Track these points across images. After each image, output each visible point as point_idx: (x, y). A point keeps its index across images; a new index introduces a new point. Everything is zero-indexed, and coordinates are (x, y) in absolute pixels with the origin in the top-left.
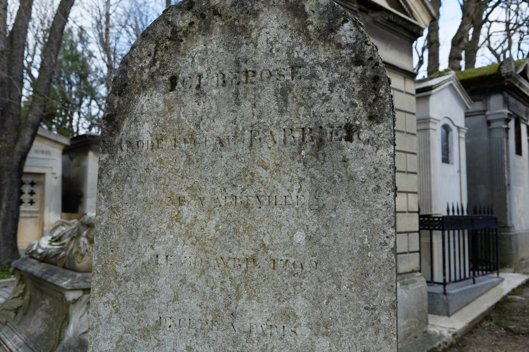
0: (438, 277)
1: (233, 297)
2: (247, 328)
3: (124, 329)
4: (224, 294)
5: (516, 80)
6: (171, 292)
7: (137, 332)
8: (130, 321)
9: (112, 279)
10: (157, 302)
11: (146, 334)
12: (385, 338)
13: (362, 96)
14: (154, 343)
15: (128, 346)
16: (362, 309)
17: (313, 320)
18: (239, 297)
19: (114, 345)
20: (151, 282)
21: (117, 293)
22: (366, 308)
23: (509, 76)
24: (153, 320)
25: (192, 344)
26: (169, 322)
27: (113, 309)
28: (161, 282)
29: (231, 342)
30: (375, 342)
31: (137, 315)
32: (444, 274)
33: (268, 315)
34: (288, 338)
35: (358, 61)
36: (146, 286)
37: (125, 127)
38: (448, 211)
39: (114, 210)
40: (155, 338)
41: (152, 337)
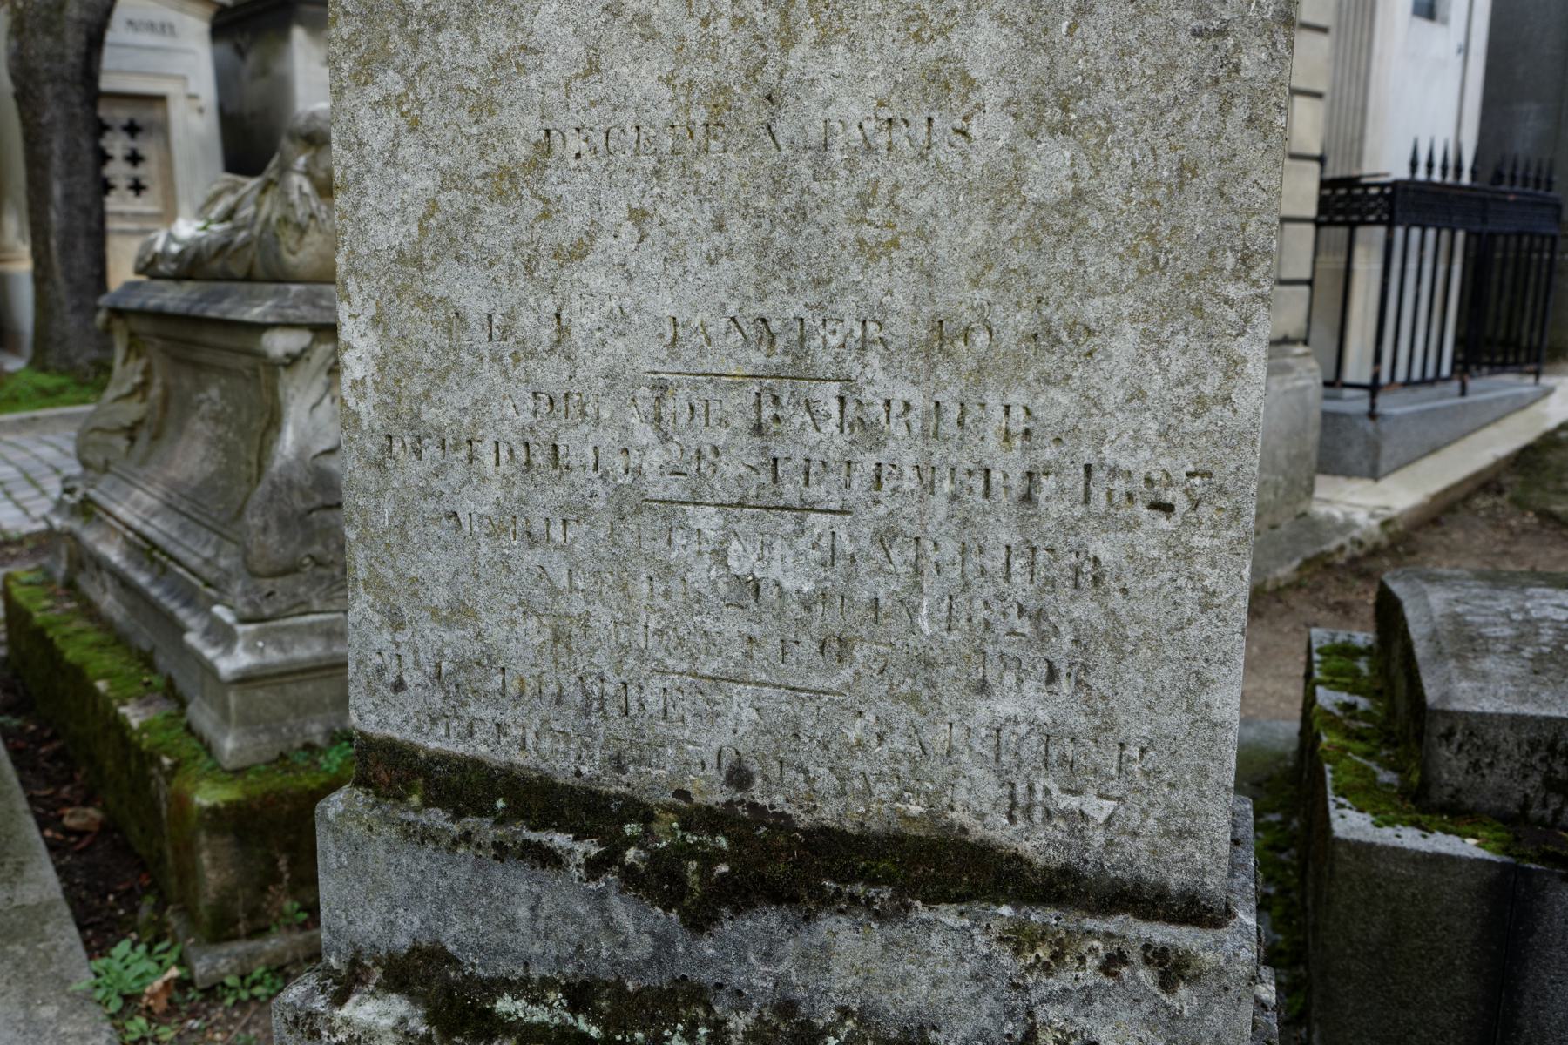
0: (1357, 368)
1: (772, 43)
2: (815, 134)
3: (439, 178)
4: (744, 35)
6: (576, 49)
7: (479, 183)
8: (457, 152)
9: (392, 26)
10: (534, 84)
11: (506, 185)
12: (1250, 121)
14: (531, 209)
15: (453, 226)
16: (1183, 37)
17: (1023, 86)
18: (789, 40)
19: (415, 230)
20: (514, 24)
21: (410, 71)
22: (1196, 33)
24: (526, 140)
25: (647, 201)
26: (575, 144)
27: (402, 122)
29: (766, 185)
30: (1214, 139)
31: (475, 130)
32: (1377, 359)
33: (882, 87)
34: (942, 153)
36: (497, 38)
38: (1414, 165)
40: (535, 195)
41: (526, 192)
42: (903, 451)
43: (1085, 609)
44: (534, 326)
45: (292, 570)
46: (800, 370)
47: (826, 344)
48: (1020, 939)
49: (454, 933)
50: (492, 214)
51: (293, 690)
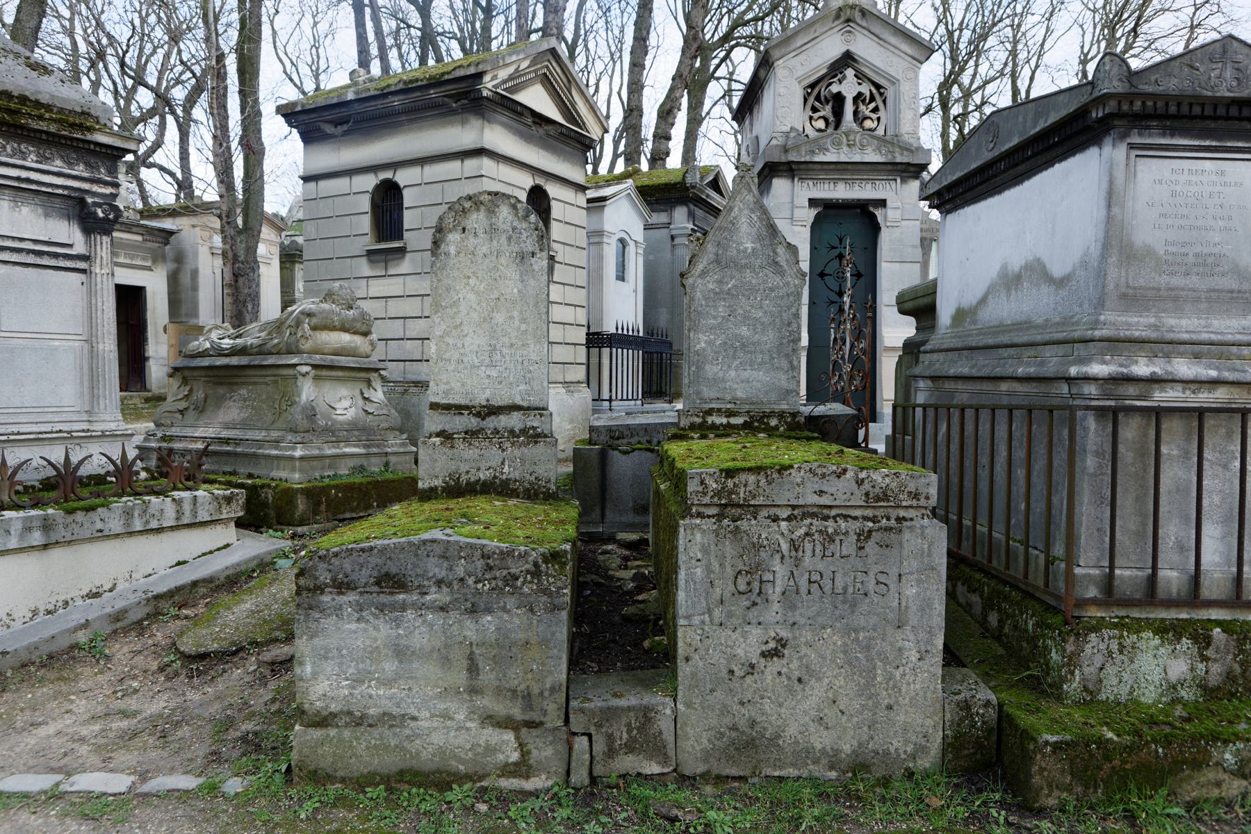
0: (606, 395)
5: (703, 192)
13: (538, 242)
23: (694, 187)
32: (611, 391)
35: (536, 229)
36: (455, 310)
37: (442, 247)
38: (617, 329)
39: (439, 281)
42: (508, 358)
43: (529, 375)
44: (460, 345)
45: (308, 431)
46: (495, 349)
47: (498, 346)
48: (524, 415)
50: (454, 331)
51: (312, 463)
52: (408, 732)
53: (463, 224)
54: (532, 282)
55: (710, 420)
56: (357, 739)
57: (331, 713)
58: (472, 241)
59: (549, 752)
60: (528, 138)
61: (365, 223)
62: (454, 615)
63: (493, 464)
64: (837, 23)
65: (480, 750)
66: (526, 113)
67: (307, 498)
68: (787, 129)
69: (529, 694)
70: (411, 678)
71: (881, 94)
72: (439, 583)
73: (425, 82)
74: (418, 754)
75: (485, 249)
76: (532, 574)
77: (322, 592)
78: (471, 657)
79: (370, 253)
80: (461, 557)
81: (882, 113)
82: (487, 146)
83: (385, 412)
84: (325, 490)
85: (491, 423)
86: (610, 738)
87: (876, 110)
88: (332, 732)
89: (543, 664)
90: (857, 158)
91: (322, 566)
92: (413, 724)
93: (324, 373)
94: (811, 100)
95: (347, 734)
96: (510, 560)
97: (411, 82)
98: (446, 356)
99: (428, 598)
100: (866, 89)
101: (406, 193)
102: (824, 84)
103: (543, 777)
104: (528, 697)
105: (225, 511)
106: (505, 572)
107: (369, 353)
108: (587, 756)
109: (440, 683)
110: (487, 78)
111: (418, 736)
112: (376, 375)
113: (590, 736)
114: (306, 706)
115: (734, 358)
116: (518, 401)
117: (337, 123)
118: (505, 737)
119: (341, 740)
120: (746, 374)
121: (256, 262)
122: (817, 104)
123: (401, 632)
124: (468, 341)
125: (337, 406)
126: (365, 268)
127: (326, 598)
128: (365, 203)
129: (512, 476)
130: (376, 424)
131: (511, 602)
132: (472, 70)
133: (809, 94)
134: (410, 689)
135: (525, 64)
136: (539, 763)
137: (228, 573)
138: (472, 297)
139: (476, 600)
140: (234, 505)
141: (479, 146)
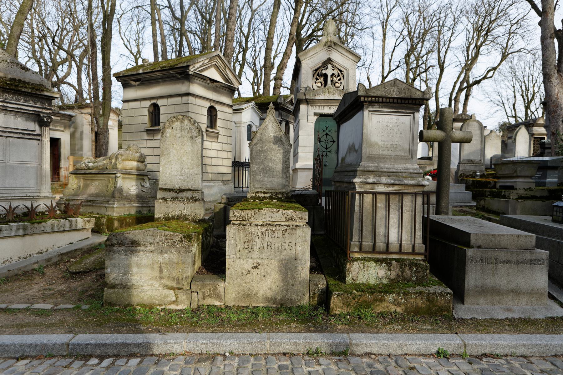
5: (285, 106)
28: (171, 155)
32: (243, 184)
44: (170, 168)
47: (184, 168)
49: (165, 196)
52: (140, 290)
53: (172, 126)
54: (196, 147)
55: (258, 195)
56: (124, 292)
57: (116, 284)
58: (175, 132)
59: (184, 297)
60: (208, 88)
61: (146, 119)
62: (155, 254)
63: (181, 209)
64: (325, 47)
65: (163, 296)
66: (207, 79)
67: (118, 221)
68: (306, 86)
69: (178, 279)
70: (141, 273)
71: (342, 74)
72: (151, 244)
73: (168, 68)
74: (143, 297)
75: (179, 135)
76: (180, 241)
77: (114, 246)
78: (160, 267)
79: (147, 131)
80: (158, 236)
81: (342, 81)
82: (191, 92)
83: (149, 191)
84: (125, 219)
85: (180, 195)
86: (204, 293)
87: (340, 80)
88: (116, 290)
89: (183, 270)
90: (332, 98)
91: (114, 238)
92: (142, 288)
93: (127, 176)
94: (316, 75)
95: (121, 291)
96: (173, 237)
97: (163, 67)
98: (165, 172)
99: (147, 248)
100: (336, 72)
101: (161, 108)
102: (321, 69)
103: (183, 305)
104: (178, 280)
105: (87, 225)
106: (171, 241)
107: (144, 169)
108: (197, 299)
109: (151, 275)
110: (191, 67)
111: (143, 292)
112: (146, 177)
113: (197, 292)
114: (108, 282)
115: (266, 173)
116: (190, 187)
117: (135, 81)
118: (171, 292)
119: (119, 293)
120: (270, 179)
121: (107, 129)
122: (318, 77)
123: (138, 259)
124: (173, 167)
125: (131, 189)
126: (146, 137)
127: (115, 248)
128: (146, 112)
129: (187, 213)
130: (146, 195)
131: (173, 250)
132: (185, 64)
133: (315, 73)
134: (141, 277)
135: (207, 61)
136: (181, 301)
137: (87, 247)
138: (175, 151)
139: (162, 249)
140: (91, 223)
141: (188, 92)
